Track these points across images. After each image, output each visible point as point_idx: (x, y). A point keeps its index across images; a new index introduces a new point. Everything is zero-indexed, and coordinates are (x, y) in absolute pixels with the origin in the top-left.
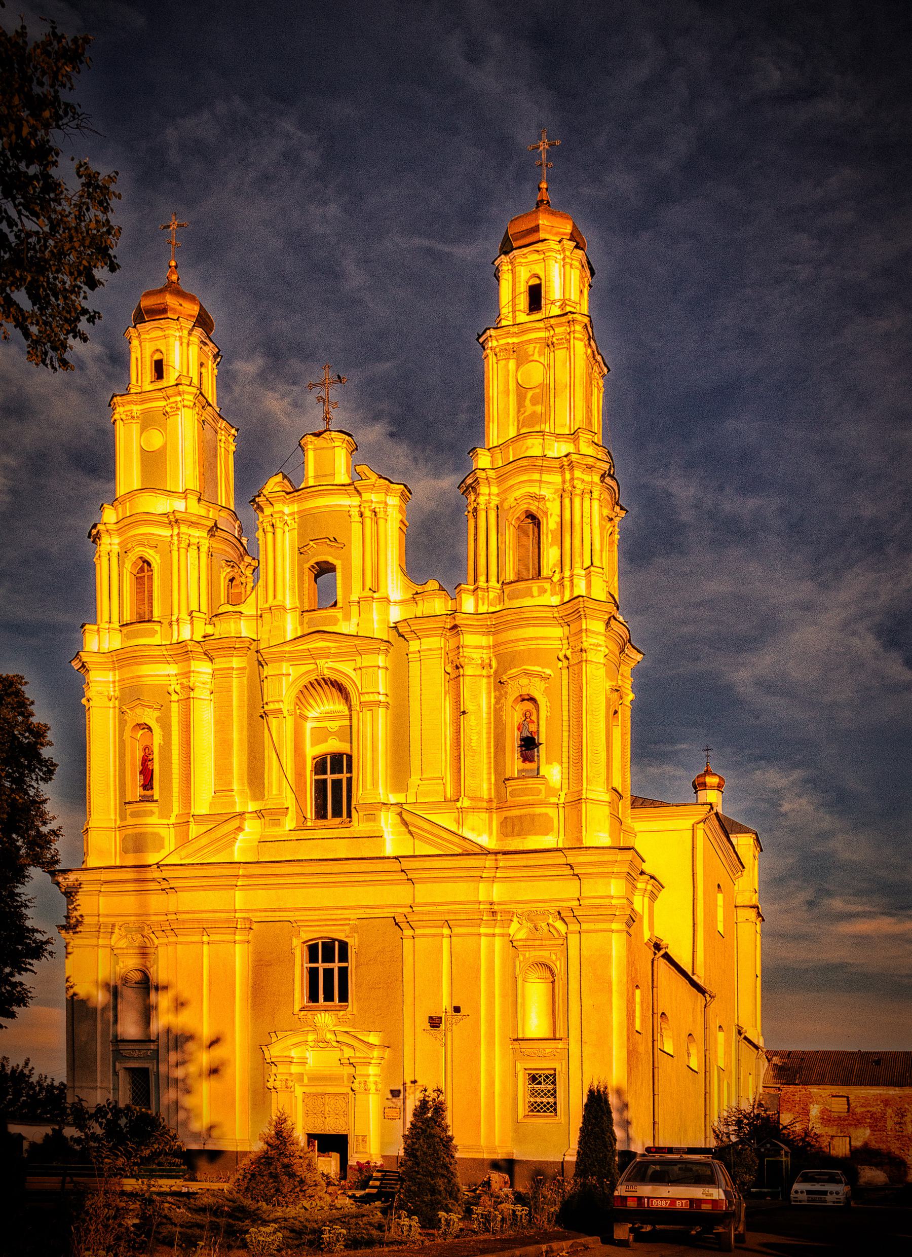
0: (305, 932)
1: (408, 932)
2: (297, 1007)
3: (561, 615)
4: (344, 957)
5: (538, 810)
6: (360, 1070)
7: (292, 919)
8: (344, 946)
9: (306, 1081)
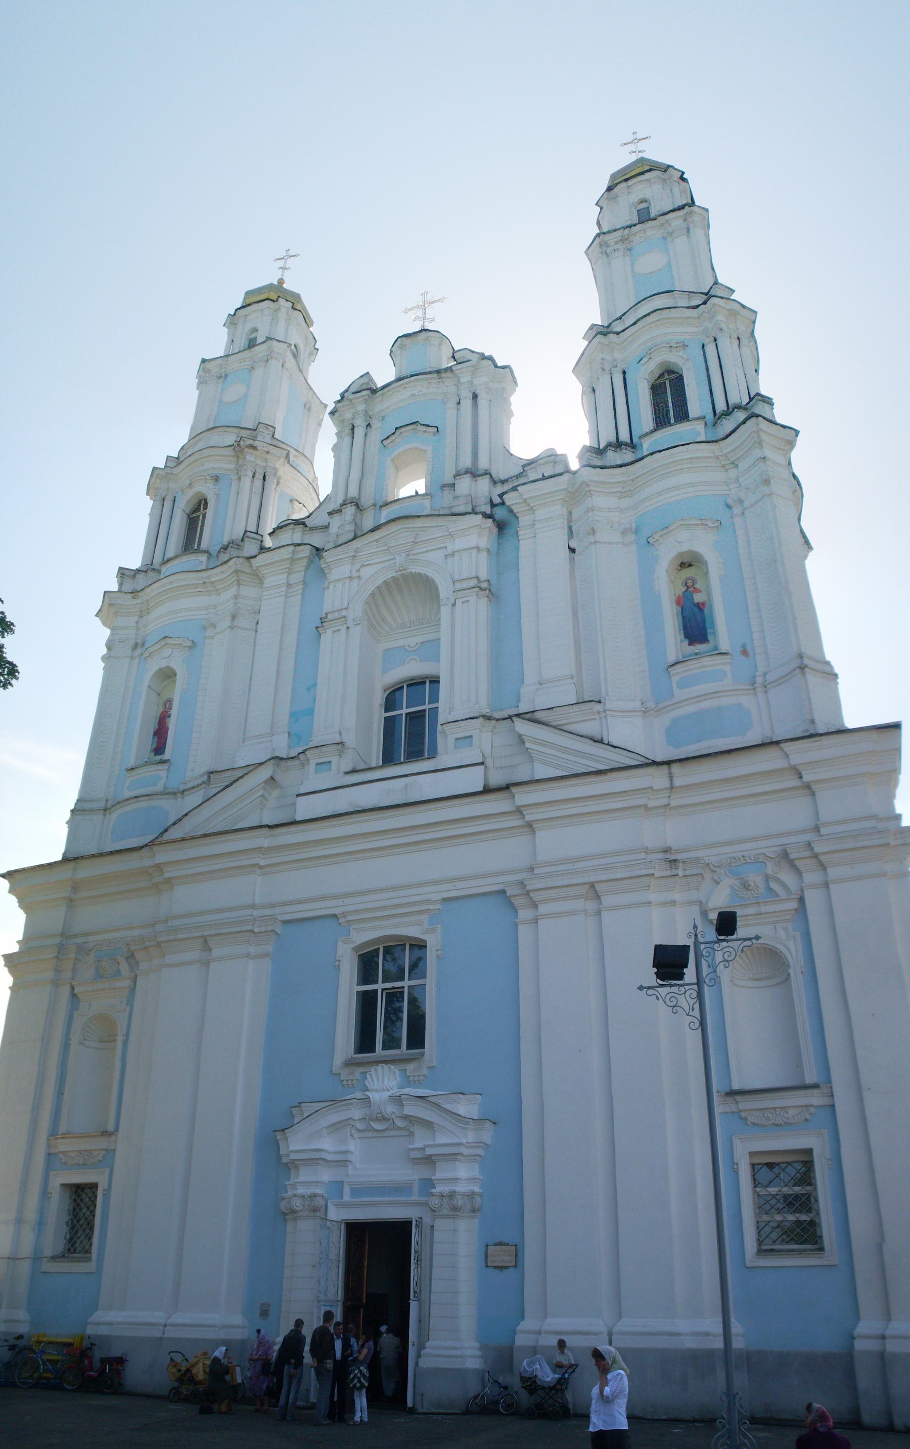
1: (525, 914)
2: (338, 1060)
3: (725, 452)
4: (417, 966)
5: (724, 701)
6: (442, 1172)
8: (419, 946)
9: (347, 1197)
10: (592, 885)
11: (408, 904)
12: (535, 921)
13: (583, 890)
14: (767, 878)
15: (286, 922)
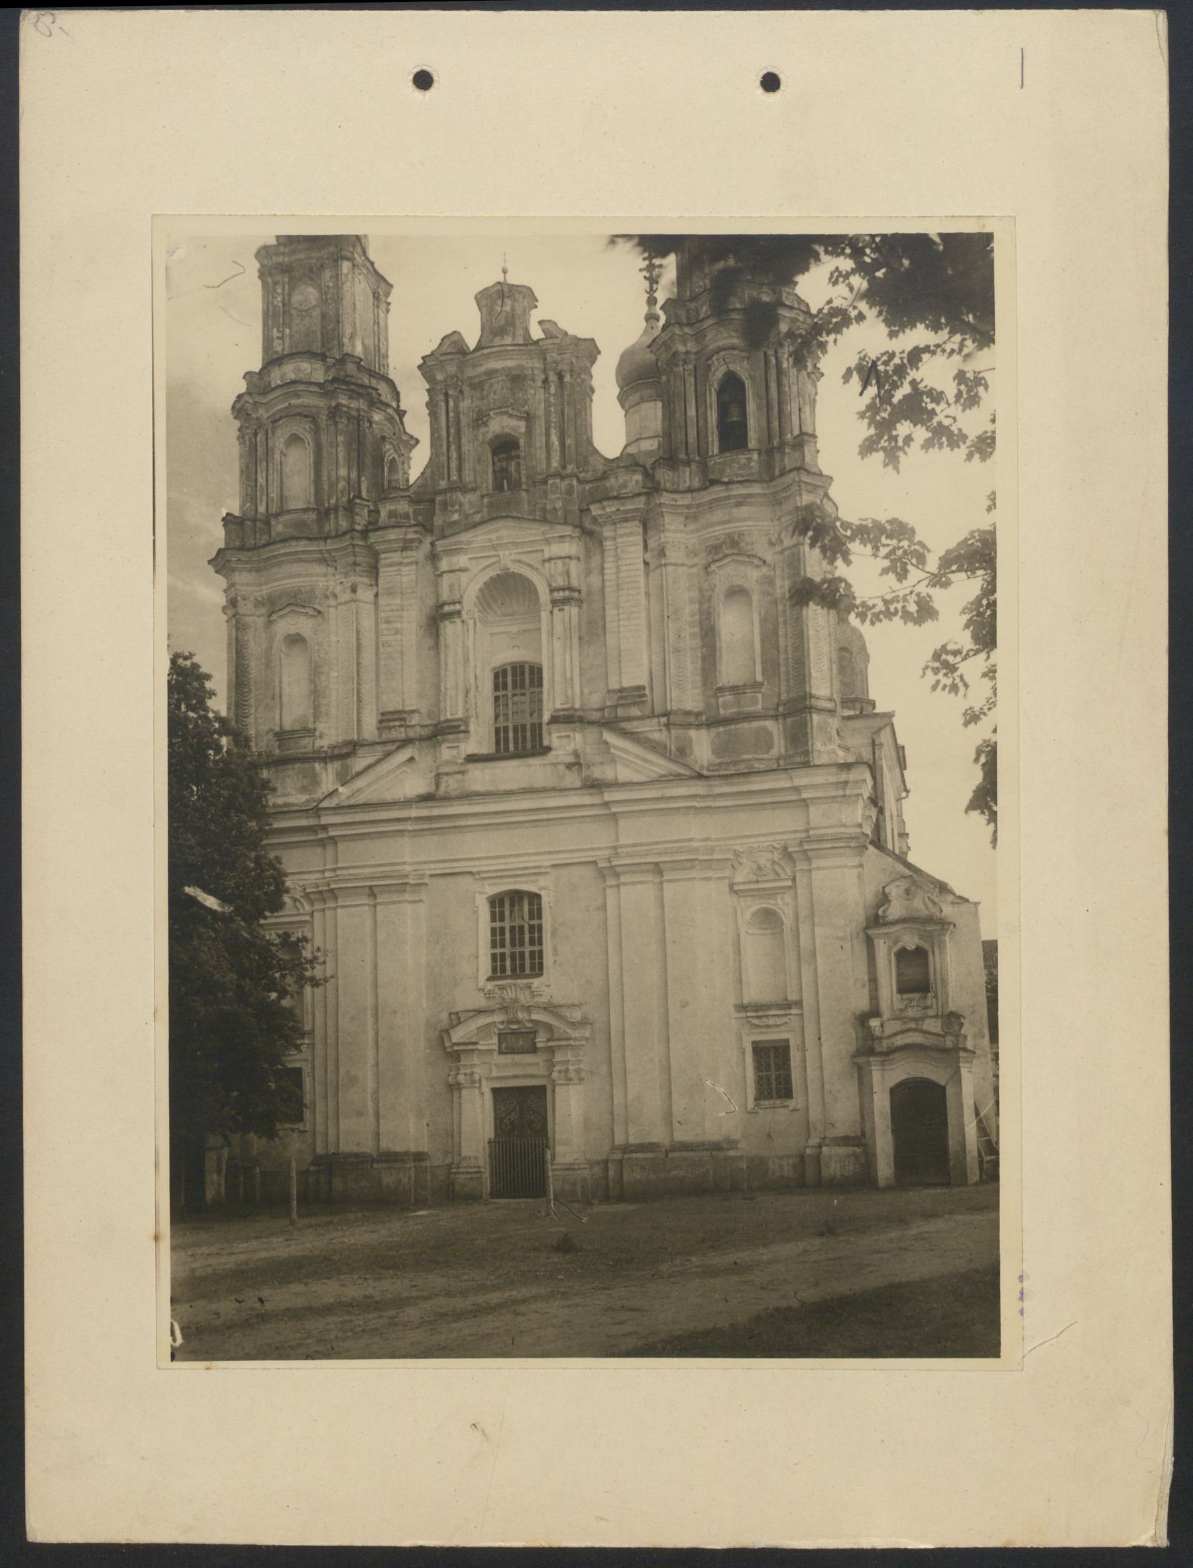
0: (490, 885)
7: (474, 870)
8: (535, 898)
10: (657, 864)
11: (527, 868)
12: (618, 886)
13: (652, 867)
14: (774, 862)
15: (431, 876)
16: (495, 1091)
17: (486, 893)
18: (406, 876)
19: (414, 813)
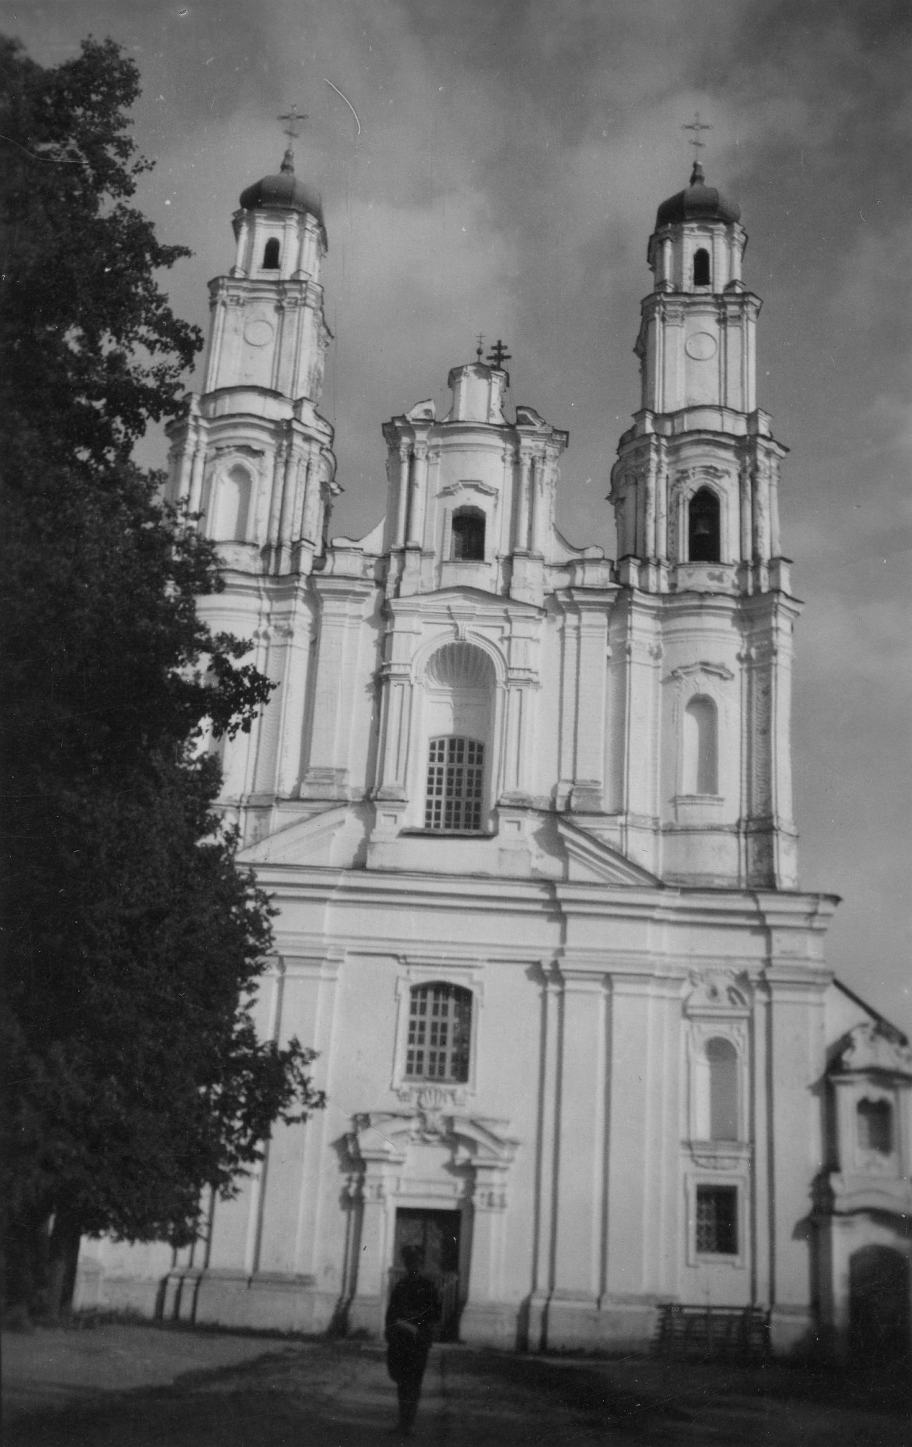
0: (417, 972)
13: (602, 977)
16: (402, 1213)
17: (410, 980)
18: (325, 950)
19: (341, 881)
